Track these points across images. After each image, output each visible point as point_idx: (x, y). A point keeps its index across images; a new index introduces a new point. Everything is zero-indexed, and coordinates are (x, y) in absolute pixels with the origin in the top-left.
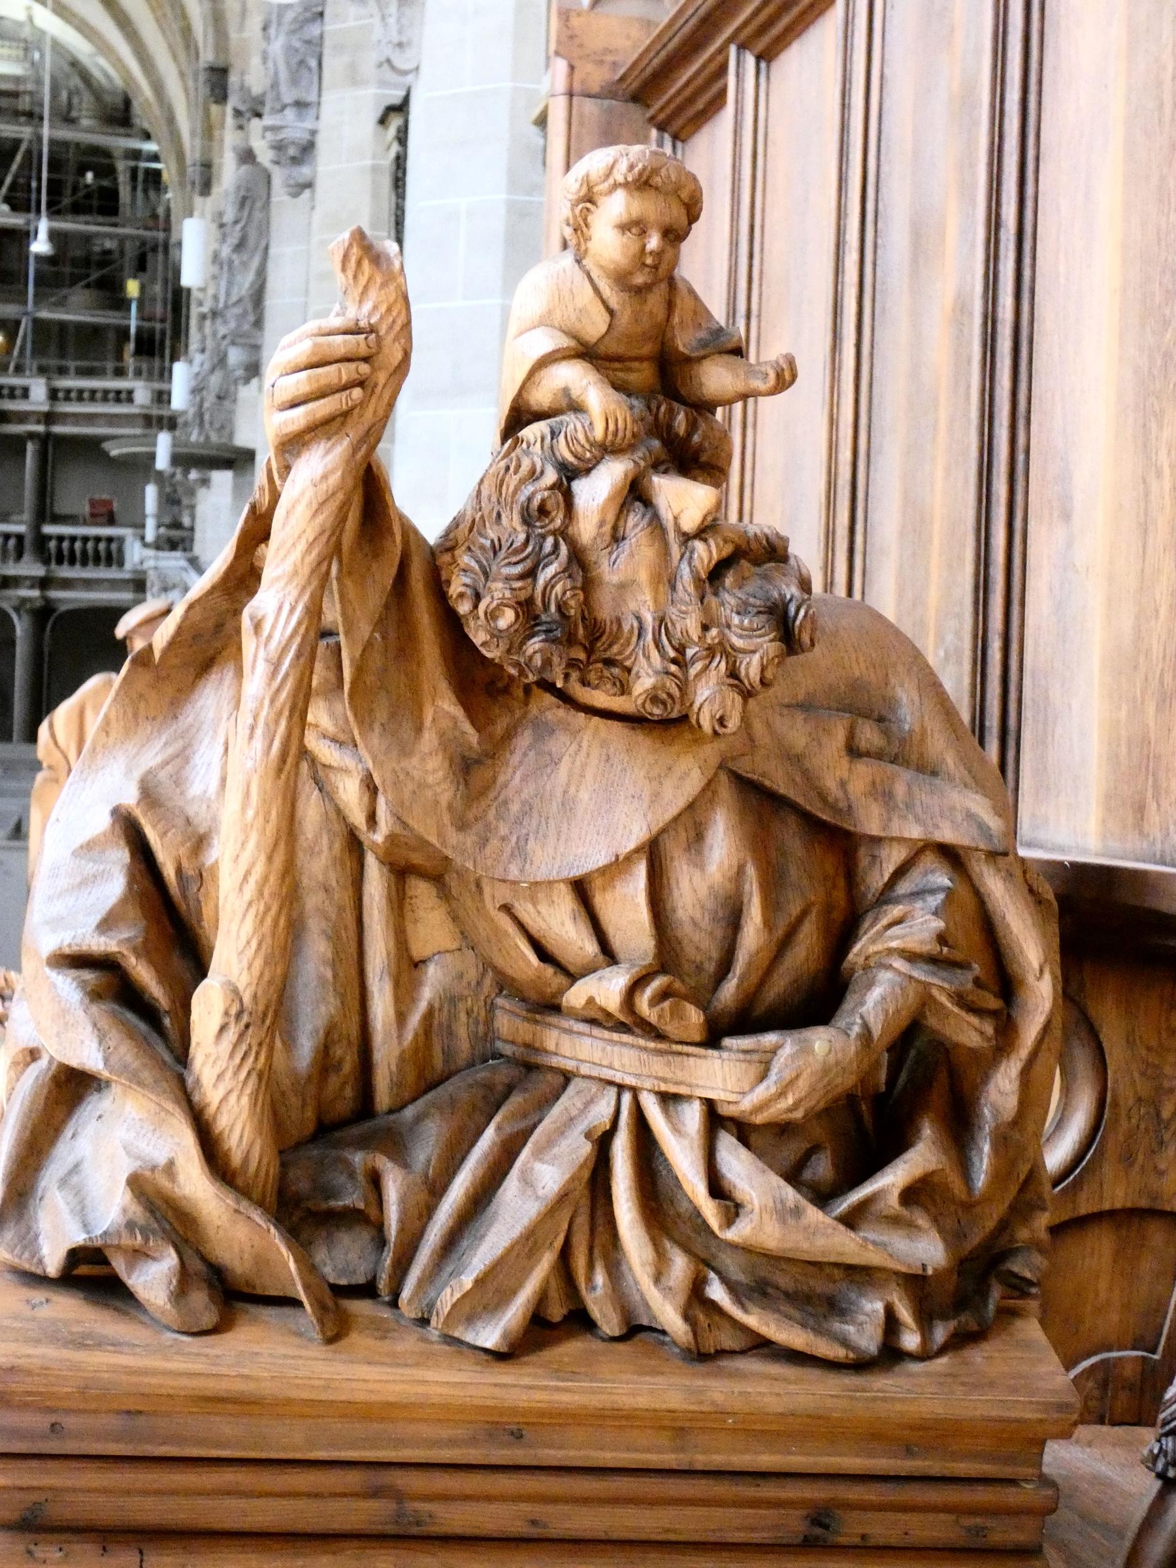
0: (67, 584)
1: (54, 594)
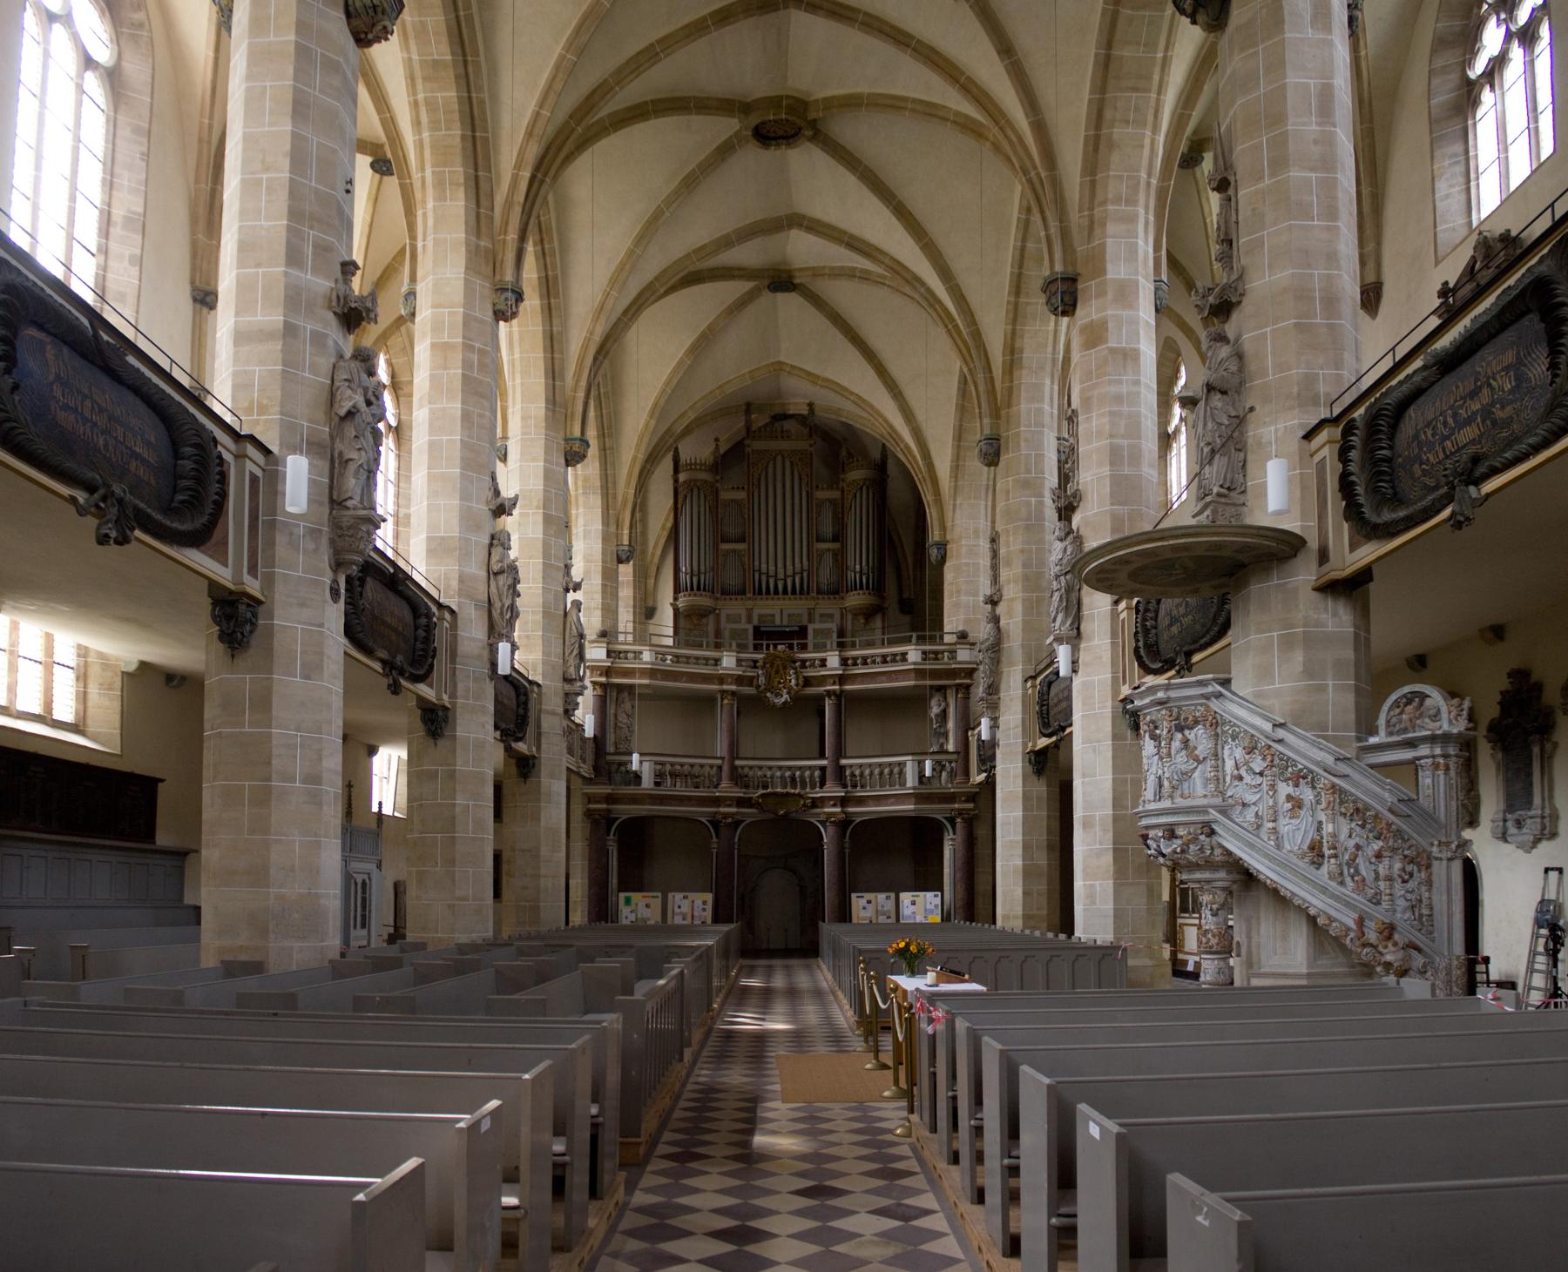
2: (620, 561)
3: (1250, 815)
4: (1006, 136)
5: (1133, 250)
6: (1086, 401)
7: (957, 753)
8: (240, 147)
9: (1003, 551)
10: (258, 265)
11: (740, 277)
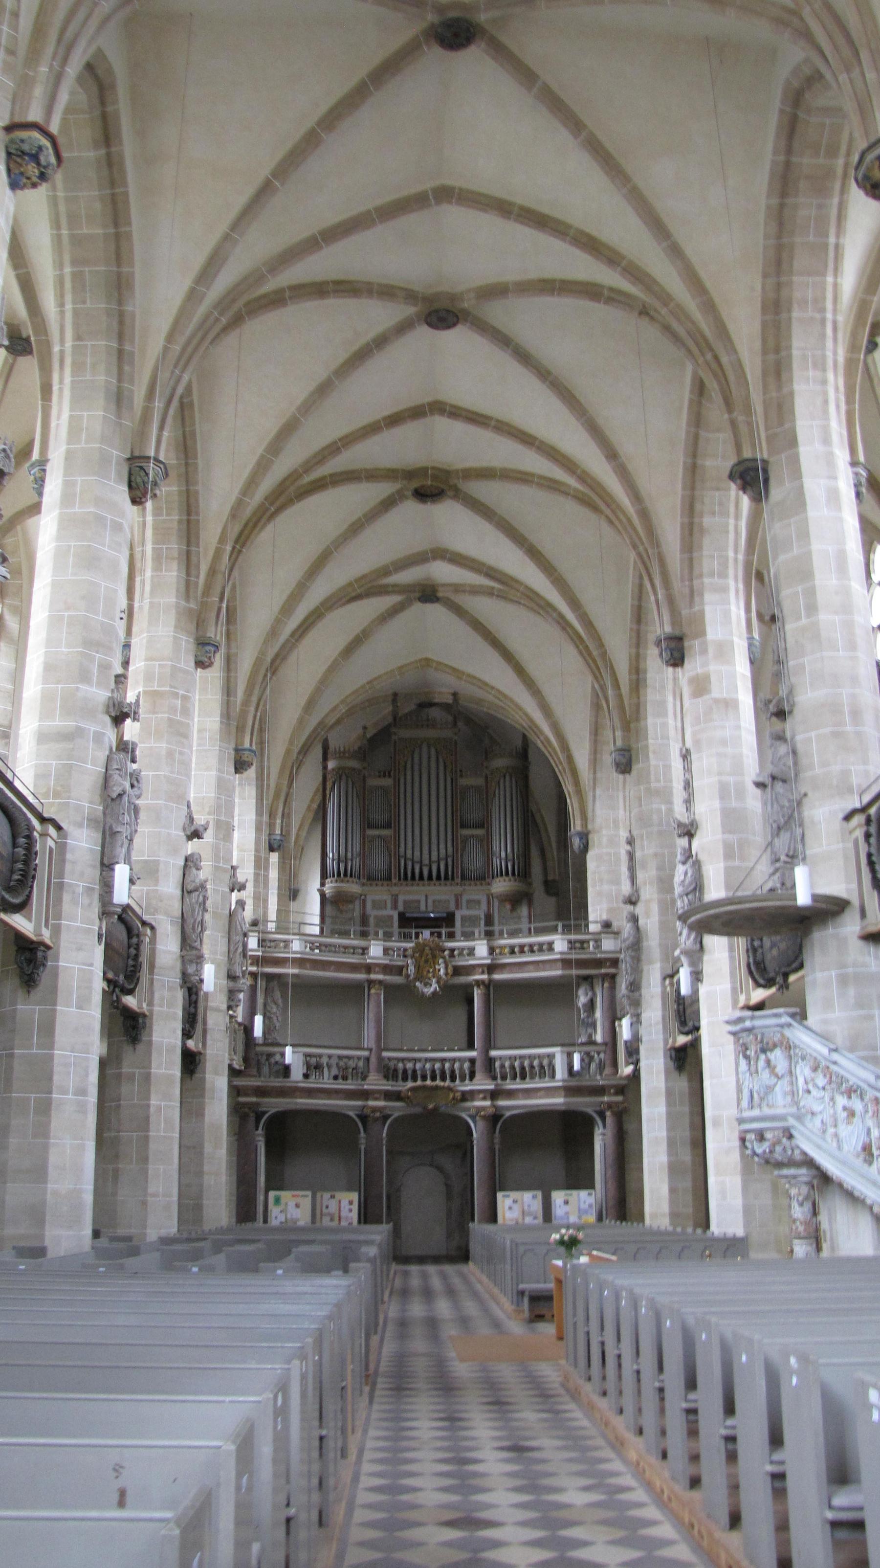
0: (511, 1094)
1: (502, 1103)
2: (272, 849)
3: (817, 1122)
4: (617, 517)
5: (727, 614)
6: (697, 742)
7: (605, 1044)
8: (48, 590)
9: (638, 854)
10: (58, 682)
11: (393, 592)
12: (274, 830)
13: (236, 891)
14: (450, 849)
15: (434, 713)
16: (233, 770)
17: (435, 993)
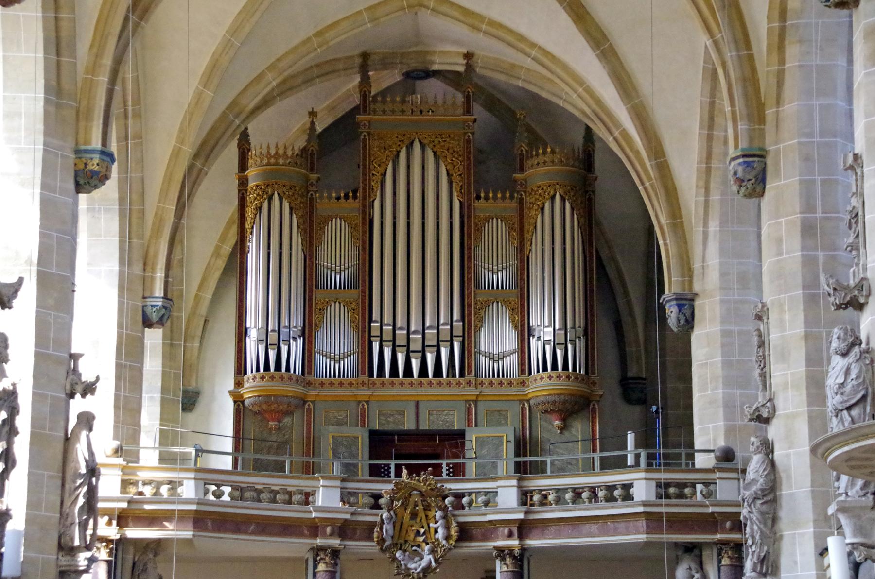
2: (147, 323)
12: (152, 291)
13: (78, 396)
14: (458, 325)
15: (434, 88)
16: (71, 186)
17: (427, 570)
